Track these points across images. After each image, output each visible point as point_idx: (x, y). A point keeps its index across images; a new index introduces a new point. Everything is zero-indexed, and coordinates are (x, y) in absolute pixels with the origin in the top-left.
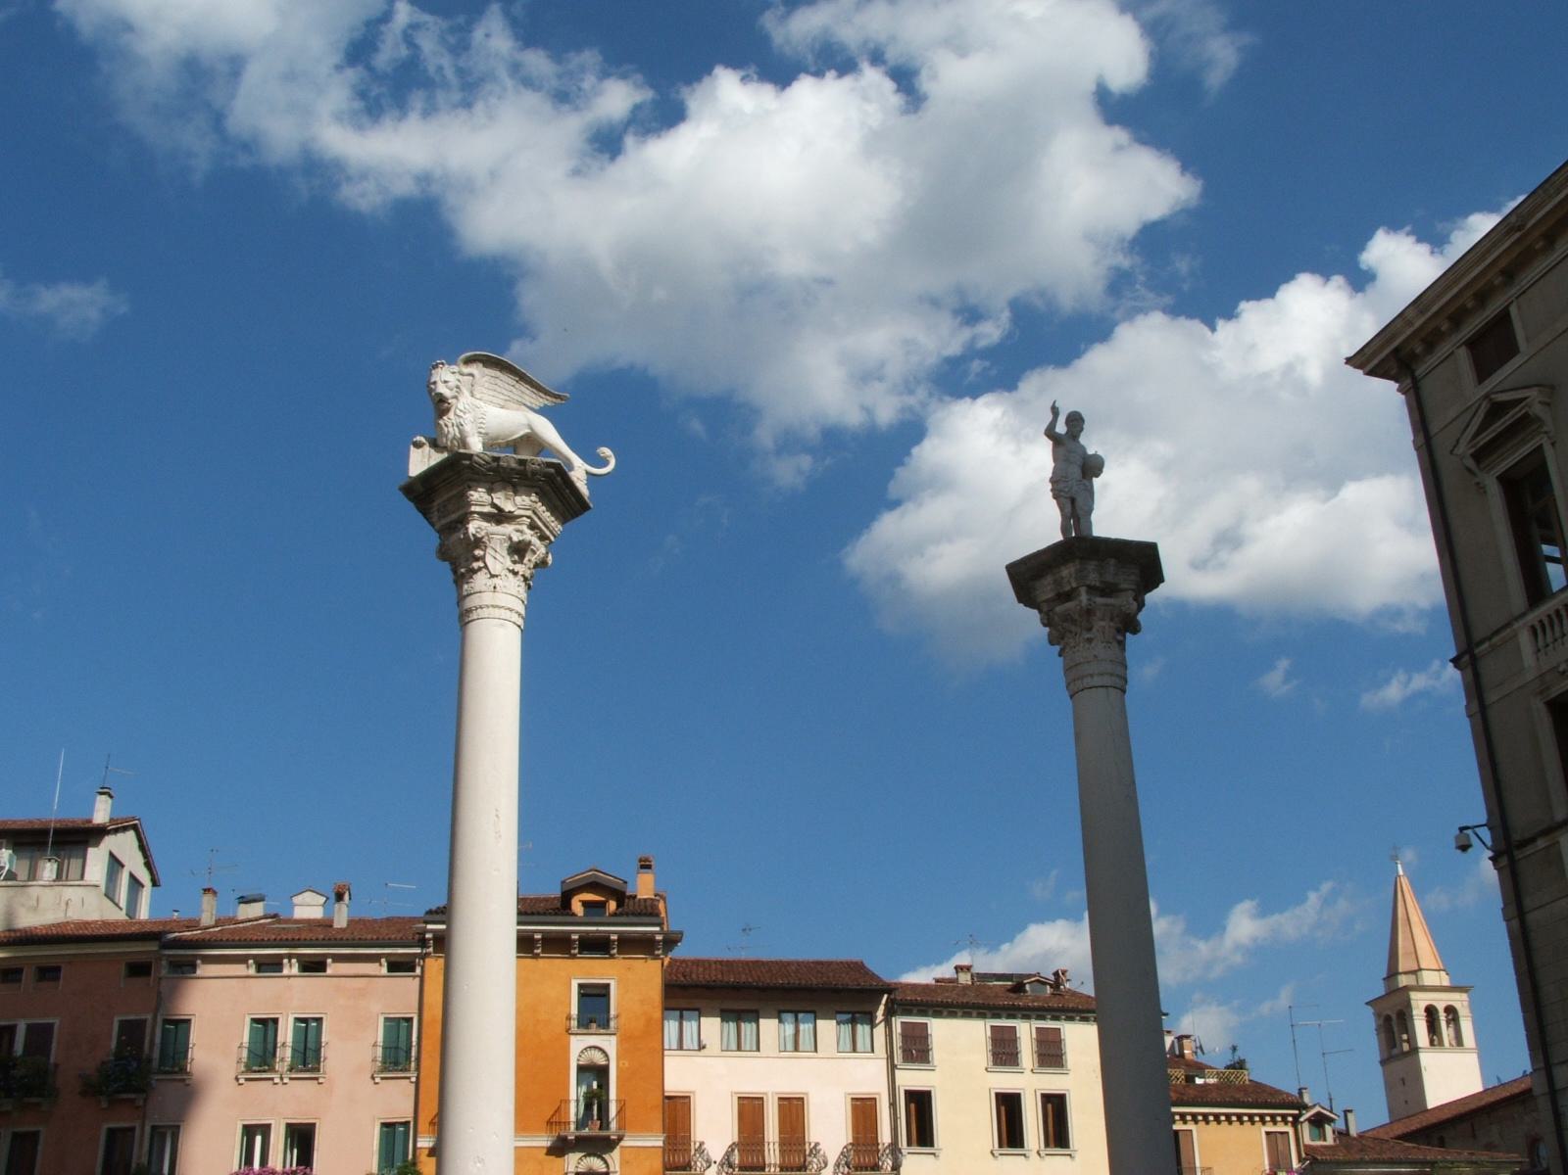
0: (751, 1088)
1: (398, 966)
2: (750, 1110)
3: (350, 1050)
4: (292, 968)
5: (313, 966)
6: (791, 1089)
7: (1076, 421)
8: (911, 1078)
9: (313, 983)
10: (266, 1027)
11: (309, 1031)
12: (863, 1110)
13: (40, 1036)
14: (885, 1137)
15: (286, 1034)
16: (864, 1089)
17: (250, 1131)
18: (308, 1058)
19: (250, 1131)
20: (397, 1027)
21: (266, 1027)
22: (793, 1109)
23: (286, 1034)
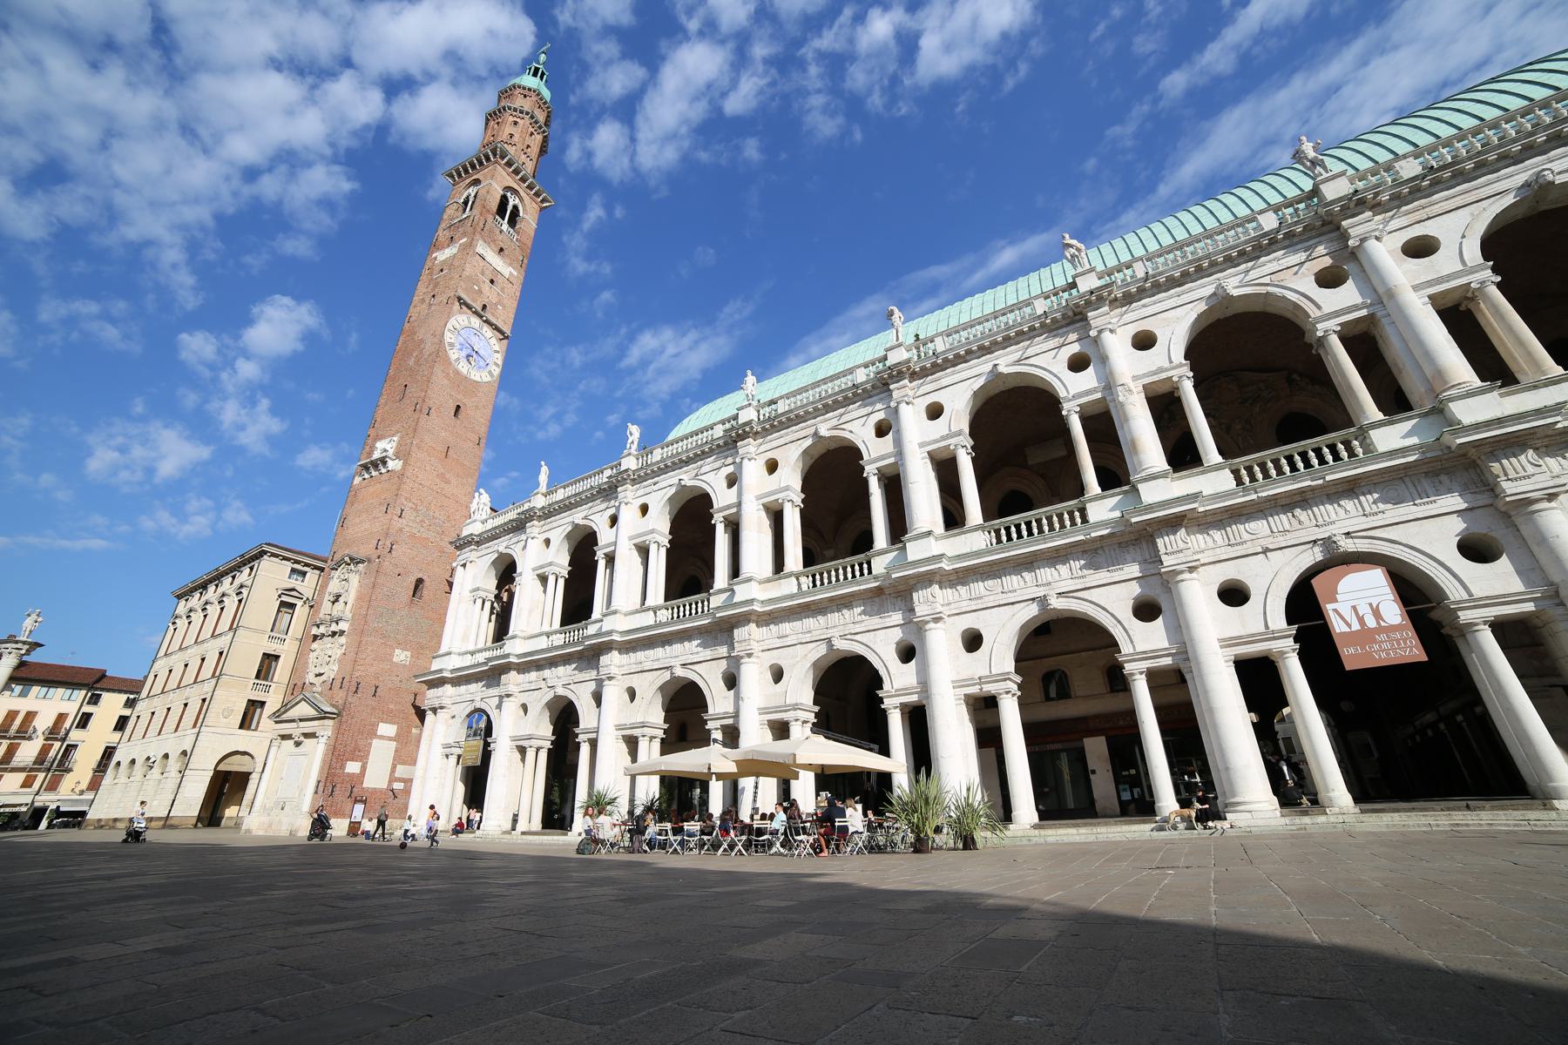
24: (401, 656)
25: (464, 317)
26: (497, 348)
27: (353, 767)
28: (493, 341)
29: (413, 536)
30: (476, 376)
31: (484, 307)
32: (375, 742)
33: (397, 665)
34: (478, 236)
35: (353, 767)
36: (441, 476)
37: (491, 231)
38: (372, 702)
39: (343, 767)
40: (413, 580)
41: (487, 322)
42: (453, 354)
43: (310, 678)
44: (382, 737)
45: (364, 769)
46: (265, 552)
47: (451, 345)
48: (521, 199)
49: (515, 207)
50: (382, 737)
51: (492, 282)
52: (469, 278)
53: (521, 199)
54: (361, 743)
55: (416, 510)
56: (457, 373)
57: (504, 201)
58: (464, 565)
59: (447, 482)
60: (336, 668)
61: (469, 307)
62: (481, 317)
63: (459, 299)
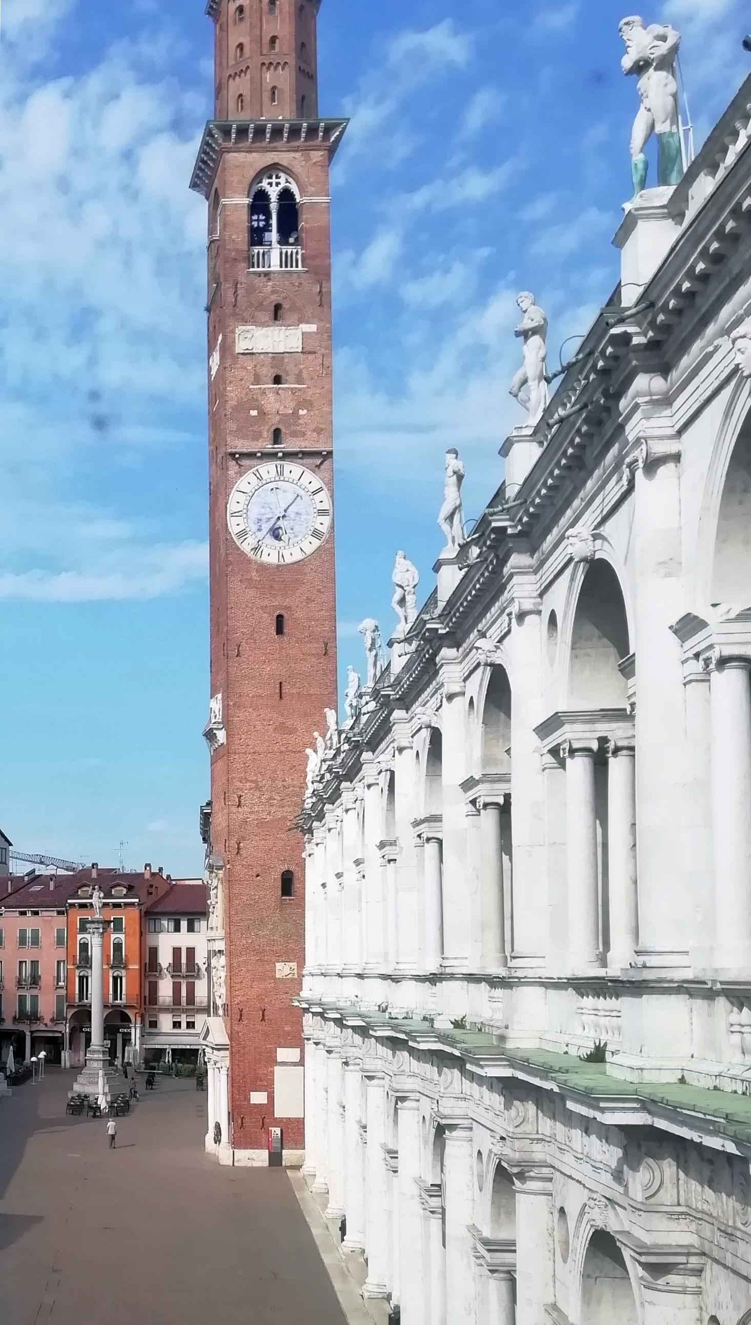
24: (283, 969)
25: (249, 476)
26: (317, 483)
27: (258, 1098)
28: (309, 476)
29: (262, 824)
30: (293, 555)
31: (277, 436)
32: (277, 1069)
34: (230, 321)
35: (258, 1098)
36: (282, 728)
37: (251, 289)
38: (261, 1027)
41: (288, 456)
42: (246, 547)
44: (284, 1064)
45: (271, 1098)
47: (243, 534)
48: (288, 171)
49: (286, 195)
50: (284, 1064)
51: (277, 380)
52: (242, 407)
53: (288, 171)
54: (260, 1072)
55: (258, 788)
56: (263, 568)
57: (259, 202)
59: (292, 731)
61: (251, 455)
62: (273, 456)
63: (232, 455)
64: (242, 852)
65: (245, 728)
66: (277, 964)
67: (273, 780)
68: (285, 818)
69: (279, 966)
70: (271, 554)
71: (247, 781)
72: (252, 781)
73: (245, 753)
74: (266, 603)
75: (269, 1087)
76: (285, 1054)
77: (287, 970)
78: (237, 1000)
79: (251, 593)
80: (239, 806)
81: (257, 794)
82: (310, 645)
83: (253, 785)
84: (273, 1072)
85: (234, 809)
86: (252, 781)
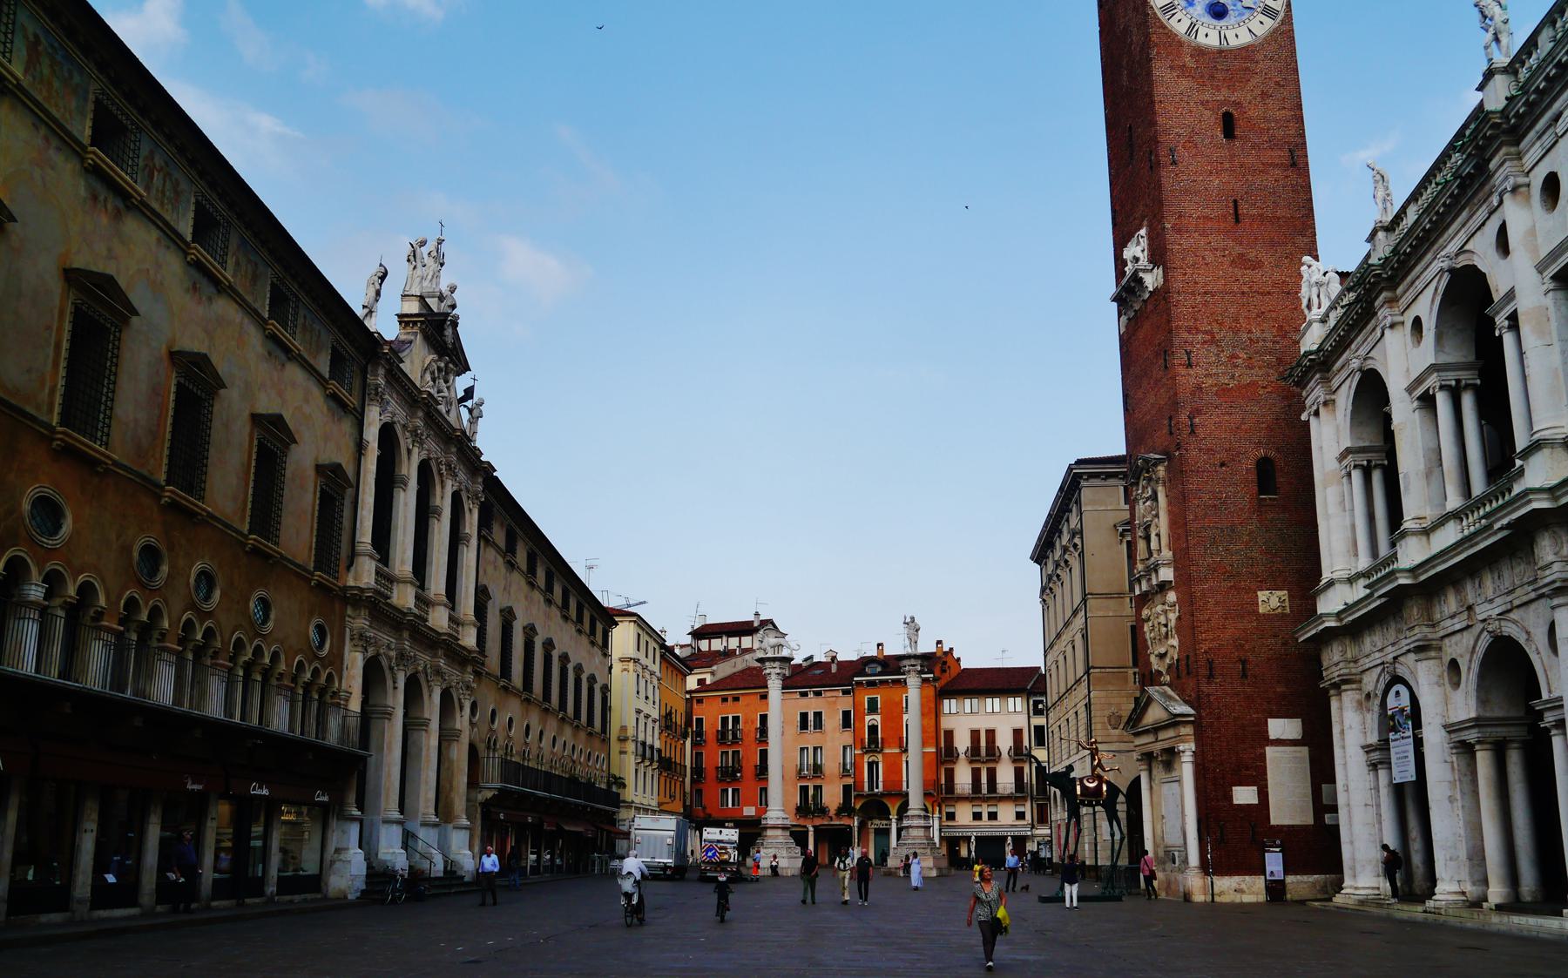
0: (975, 727)
1: (845, 692)
2: (975, 734)
3: (832, 721)
4: (811, 695)
5: (818, 694)
6: (991, 726)
7: (913, 619)
8: (1039, 721)
9: (819, 700)
10: (804, 716)
11: (818, 715)
12: (1017, 733)
13: (736, 719)
14: (1026, 743)
15: (811, 717)
16: (1018, 726)
17: (802, 749)
18: (818, 724)
19: (802, 749)
20: (846, 714)
21: (804, 716)
22: (991, 734)
23: (811, 717)
24: (1270, 600)
29: (1223, 391)
32: (1270, 752)
33: (1267, 617)
39: (1229, 797)
40: (1248, 464)
43: (1155, 664)
46: (1080, 476)
50: (1279, 742)
55: (1213, 341)
58: (1317, 414)
60: (1175, 642)
64: (1201, 432)
65: (1190, 260)
66: (1262, 595)
67: (1236, 332)
68: (1253, 384)
69: (1262, 595)
70: (1209, 36)
71: (1198, 331)
72: (1206, 332)
73: (1193, 294)
74: (1207, 97)
75: (1258, 778)
76: (1280, 728)
77: (1274, 602)
78: (1204, 647)
79: (1185, 84)
80: (1190, 365)
81: (1213, 349)
82: (1270, 153)
83: (1208, 337)
84: (1263, 757)
85: (1182, 370)
86: (1206, 332)
